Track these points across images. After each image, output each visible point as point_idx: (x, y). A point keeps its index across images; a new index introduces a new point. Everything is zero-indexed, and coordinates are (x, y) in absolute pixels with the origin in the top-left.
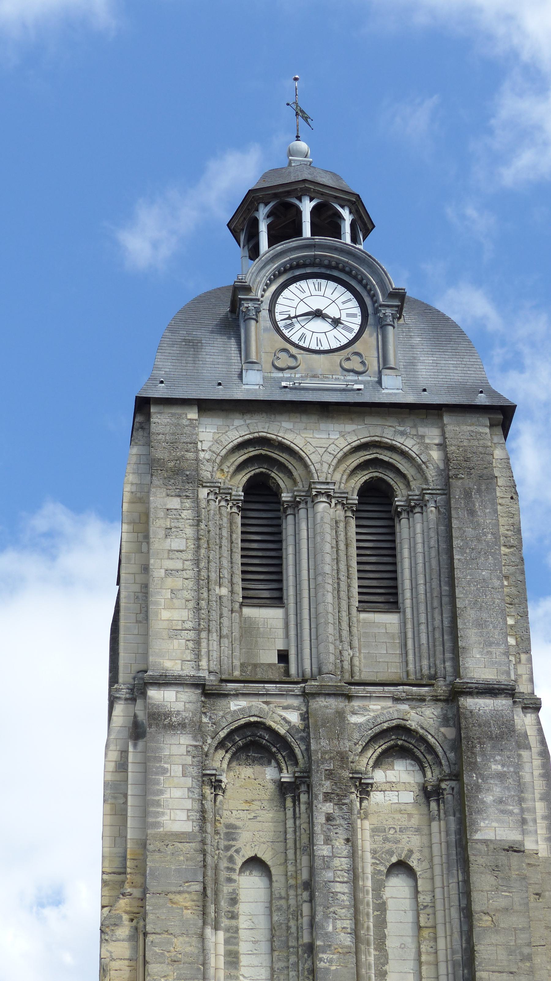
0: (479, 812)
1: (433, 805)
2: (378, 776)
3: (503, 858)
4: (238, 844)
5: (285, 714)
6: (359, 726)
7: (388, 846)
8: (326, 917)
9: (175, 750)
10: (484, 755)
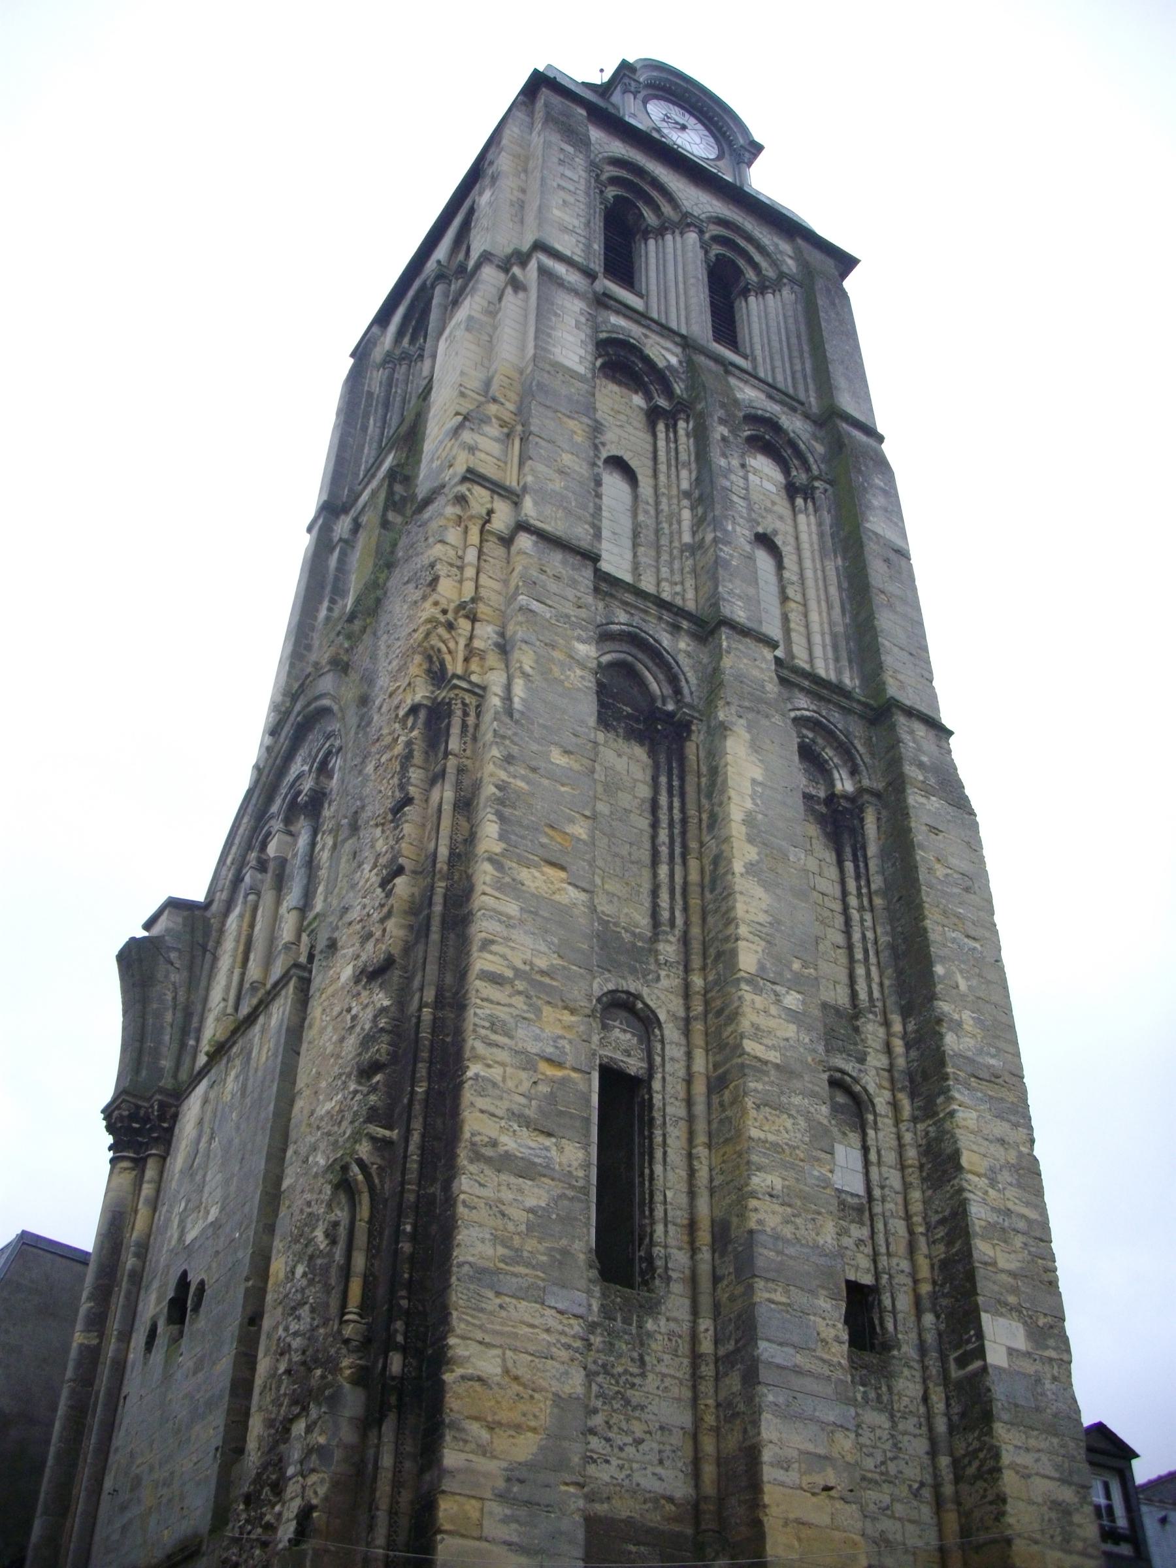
1: (799, 501)
3: (893, 556)
4: (603, 439)
5: (664, 352)
8: (726, 517)
9: (568, 304)
10: (867, 466)
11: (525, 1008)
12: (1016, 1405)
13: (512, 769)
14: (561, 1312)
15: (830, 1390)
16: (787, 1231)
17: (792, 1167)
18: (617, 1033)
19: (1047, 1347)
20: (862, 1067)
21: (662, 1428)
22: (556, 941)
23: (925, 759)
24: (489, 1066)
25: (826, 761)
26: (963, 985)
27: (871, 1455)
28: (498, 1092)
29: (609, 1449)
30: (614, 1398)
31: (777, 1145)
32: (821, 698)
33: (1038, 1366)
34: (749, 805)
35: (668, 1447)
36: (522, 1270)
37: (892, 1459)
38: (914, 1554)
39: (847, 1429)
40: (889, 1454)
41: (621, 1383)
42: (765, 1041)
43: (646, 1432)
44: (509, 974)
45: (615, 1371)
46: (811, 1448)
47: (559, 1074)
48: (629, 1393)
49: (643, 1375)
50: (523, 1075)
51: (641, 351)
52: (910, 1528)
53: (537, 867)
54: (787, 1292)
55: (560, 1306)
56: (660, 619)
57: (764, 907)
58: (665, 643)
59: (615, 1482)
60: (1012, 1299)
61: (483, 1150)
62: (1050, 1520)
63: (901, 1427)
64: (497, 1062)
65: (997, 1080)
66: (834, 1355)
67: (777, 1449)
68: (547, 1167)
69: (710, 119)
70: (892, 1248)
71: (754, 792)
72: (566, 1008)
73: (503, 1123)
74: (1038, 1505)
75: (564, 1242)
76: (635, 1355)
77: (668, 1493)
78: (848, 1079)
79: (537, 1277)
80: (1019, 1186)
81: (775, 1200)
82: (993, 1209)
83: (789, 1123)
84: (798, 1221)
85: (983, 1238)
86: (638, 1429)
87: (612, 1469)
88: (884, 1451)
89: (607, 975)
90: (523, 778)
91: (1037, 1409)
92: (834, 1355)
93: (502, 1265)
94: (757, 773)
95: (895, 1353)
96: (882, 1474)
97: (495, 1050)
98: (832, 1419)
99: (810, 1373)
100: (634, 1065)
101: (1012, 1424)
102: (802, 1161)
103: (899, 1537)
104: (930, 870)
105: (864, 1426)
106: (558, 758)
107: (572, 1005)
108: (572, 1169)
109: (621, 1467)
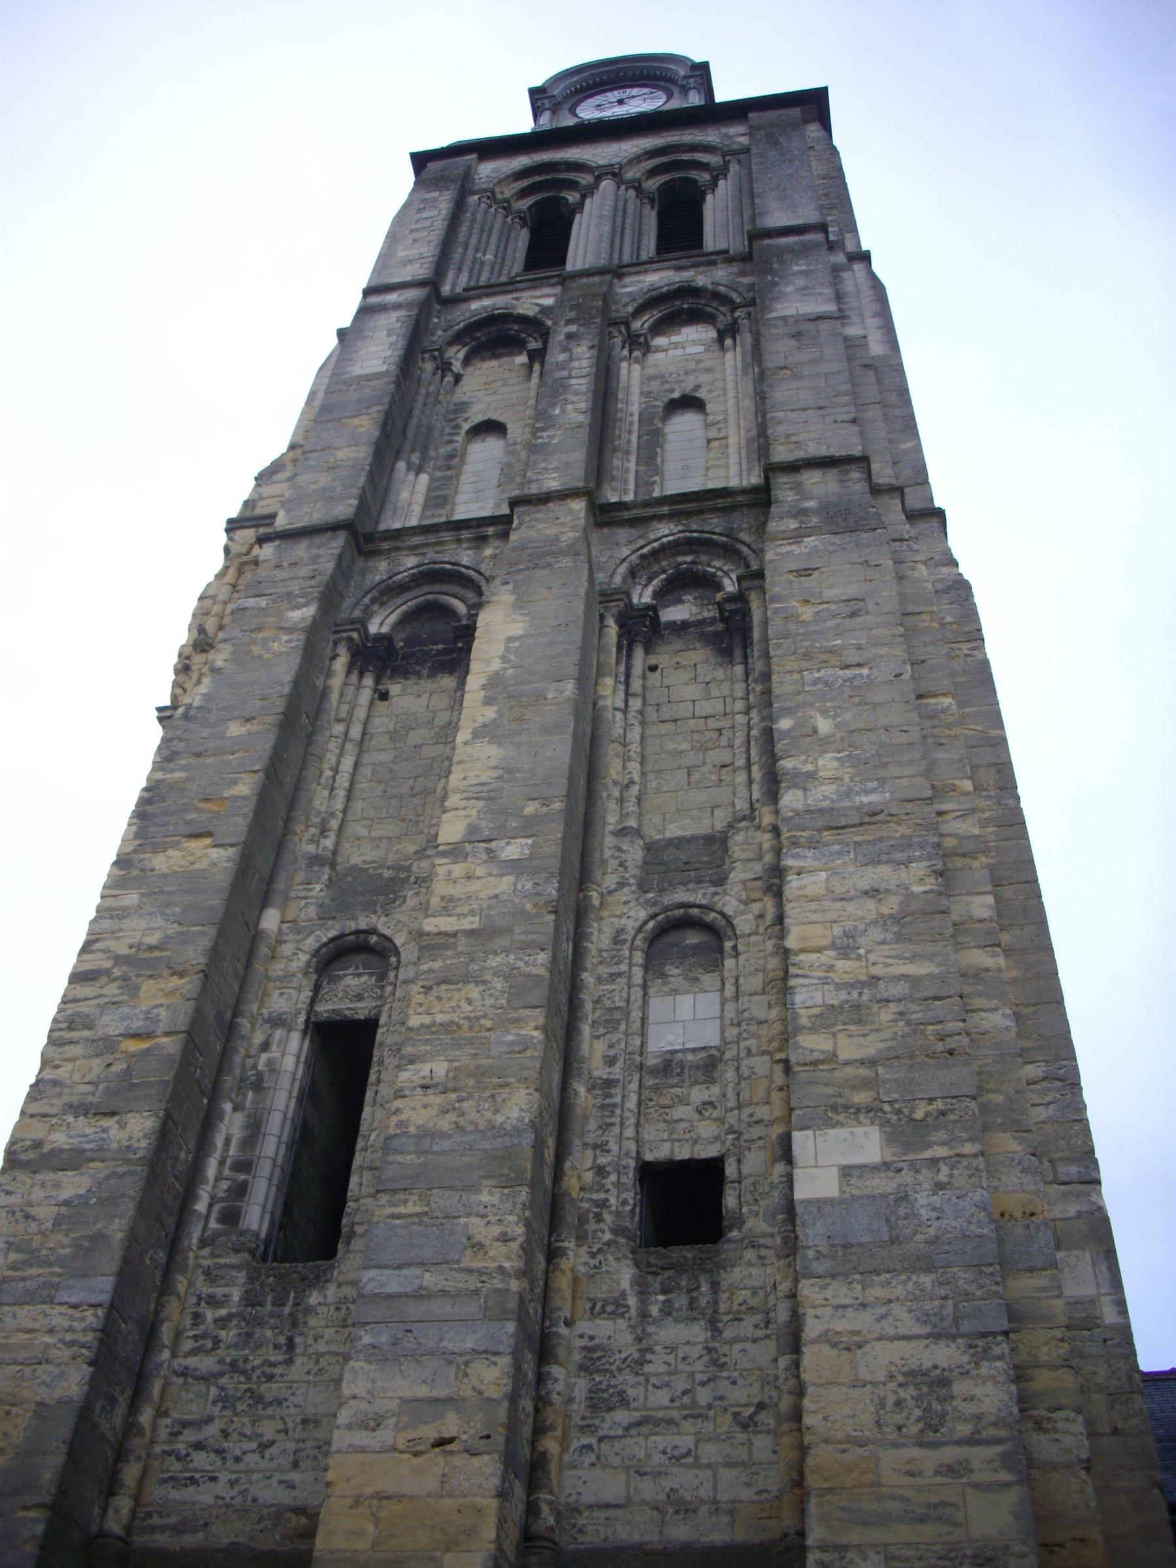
0: (776, 299)
2: (660, 341)
6: (630, 294)
7: (667, 386)
11: (117, 992)
12: (845, 1246)
13: (171, 765)
14: (75, 1306)
15: (472, 1308)
16: (445, 1124)
17: (471, 1042)
18: (349, 981)
19: (929, 1145)
20: (719, 889)
21: (305, 1422)
22: (178, 910)
23: (811, 504)
24: (57, 1067)
25: (714, 575)
26: (824, 726)
27: (667, 1384)
28: (58, 1090)
29: (219, 1463)
30: (239, 1399)
31: (452, 1022)
32: (688, 514)
33: (907, 1177)
34: (496, 665)
35: (310, 1444)
36: (34, 1271)
37: (703, 1384)
38: (731, 1512)
39: (496, 1354)
40: (699, 1377)
41: (254, 1378)
42: (459, 910)
43: (279, 1432)
44: (108, 964)
45: (248, 1366)
46: (423, 1392)
47: (144, 1045)
48: (263, 1387)
49: (290, 1361)
50: (96, 1062)
51: (511, 315)
52: (726, 1474)
53: (174, 846)
54: (425, 1199)
55: (74, 1300)
56: (459, 541)
57: (493, 763)
58: (465, 560)
59: (221, 1502)
60: (861, 1098)
61: (23, 1157)
62: (898, 1403)
63: (728, 1334)
64: (67, 1060)
65: (882, 817)
66: (494, 1259)
67: (364, 1406)
68: (101, 1149)
69: (642, 78)
70: (745, 1095)
71: (507, 649)
72: (174, 974)
73: (55, 1120)
74: (875, 1384)
75: (99, 1226)
76: (282, 1340)
77: (299, 1503)
78: (696, 911)
79: (53, 1274)
80: (899, 938)
81: (430, 1091)
82: (838, 986)
83: (474, 991)
84: (465, 1105)
85: (813, 1030)
86: (268, 1429)
87: (221, 1488)
88: (692, 1375)
89: (330, 923)
90: (183, 768)
91: (893, 1241)
92: (494, 1259)
93: (11, 1273)
94: (517, 629)
95: (734, 1234)
96: (683, 1407)
97: (67, 1048)
98: (469, 1345)
99: (444, 1293)
100: (362, 1010)
101: (833, 1276)
102: (489, 1030)
103: (704, 1493)
104: (790, 617)
105: (658, 1348)
106: (236, 729)
107: (180, 968)
108: (133, 1142)
109: (232, 1483)
